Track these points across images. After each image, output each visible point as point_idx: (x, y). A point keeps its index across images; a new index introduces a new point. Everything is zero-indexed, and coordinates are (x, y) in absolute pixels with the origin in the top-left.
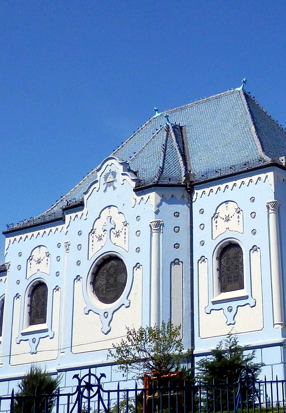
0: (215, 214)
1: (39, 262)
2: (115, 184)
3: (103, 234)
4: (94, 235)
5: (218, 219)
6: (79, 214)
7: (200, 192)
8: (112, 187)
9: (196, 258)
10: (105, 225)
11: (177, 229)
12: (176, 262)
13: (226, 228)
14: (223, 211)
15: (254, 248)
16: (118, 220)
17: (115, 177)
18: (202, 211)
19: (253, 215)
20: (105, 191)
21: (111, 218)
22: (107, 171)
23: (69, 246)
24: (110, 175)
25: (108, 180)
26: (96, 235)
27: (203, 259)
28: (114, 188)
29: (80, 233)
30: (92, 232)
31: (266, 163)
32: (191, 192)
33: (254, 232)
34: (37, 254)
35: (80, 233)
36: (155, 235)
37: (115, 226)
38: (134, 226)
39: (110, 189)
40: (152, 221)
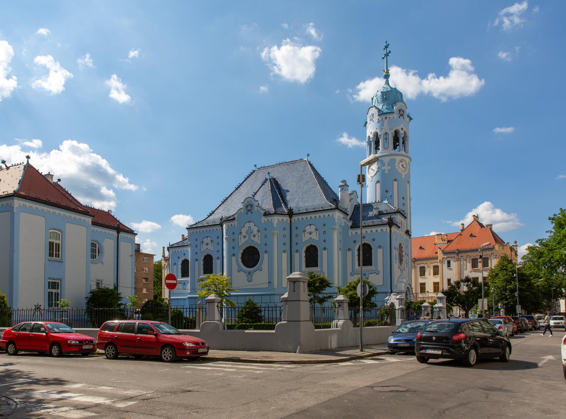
1: (207, 244)
5: (306, 233)
6: (233, 223)
9: (294, 250)
11: (284, 236)
12: (284, 251)
14: (308, 229)
15: (325, 249)
16: (255, 229)
17: (252, 207)
19: (324, 232)
25: (248, 208)
27: (297, 251)
29: (233, 233)
30: (241, 233)
31: (332, 207)
32: (291, 217)
33: (325, 241)
34: (206, 241)
35: (233, 233)
39: (250, 213)
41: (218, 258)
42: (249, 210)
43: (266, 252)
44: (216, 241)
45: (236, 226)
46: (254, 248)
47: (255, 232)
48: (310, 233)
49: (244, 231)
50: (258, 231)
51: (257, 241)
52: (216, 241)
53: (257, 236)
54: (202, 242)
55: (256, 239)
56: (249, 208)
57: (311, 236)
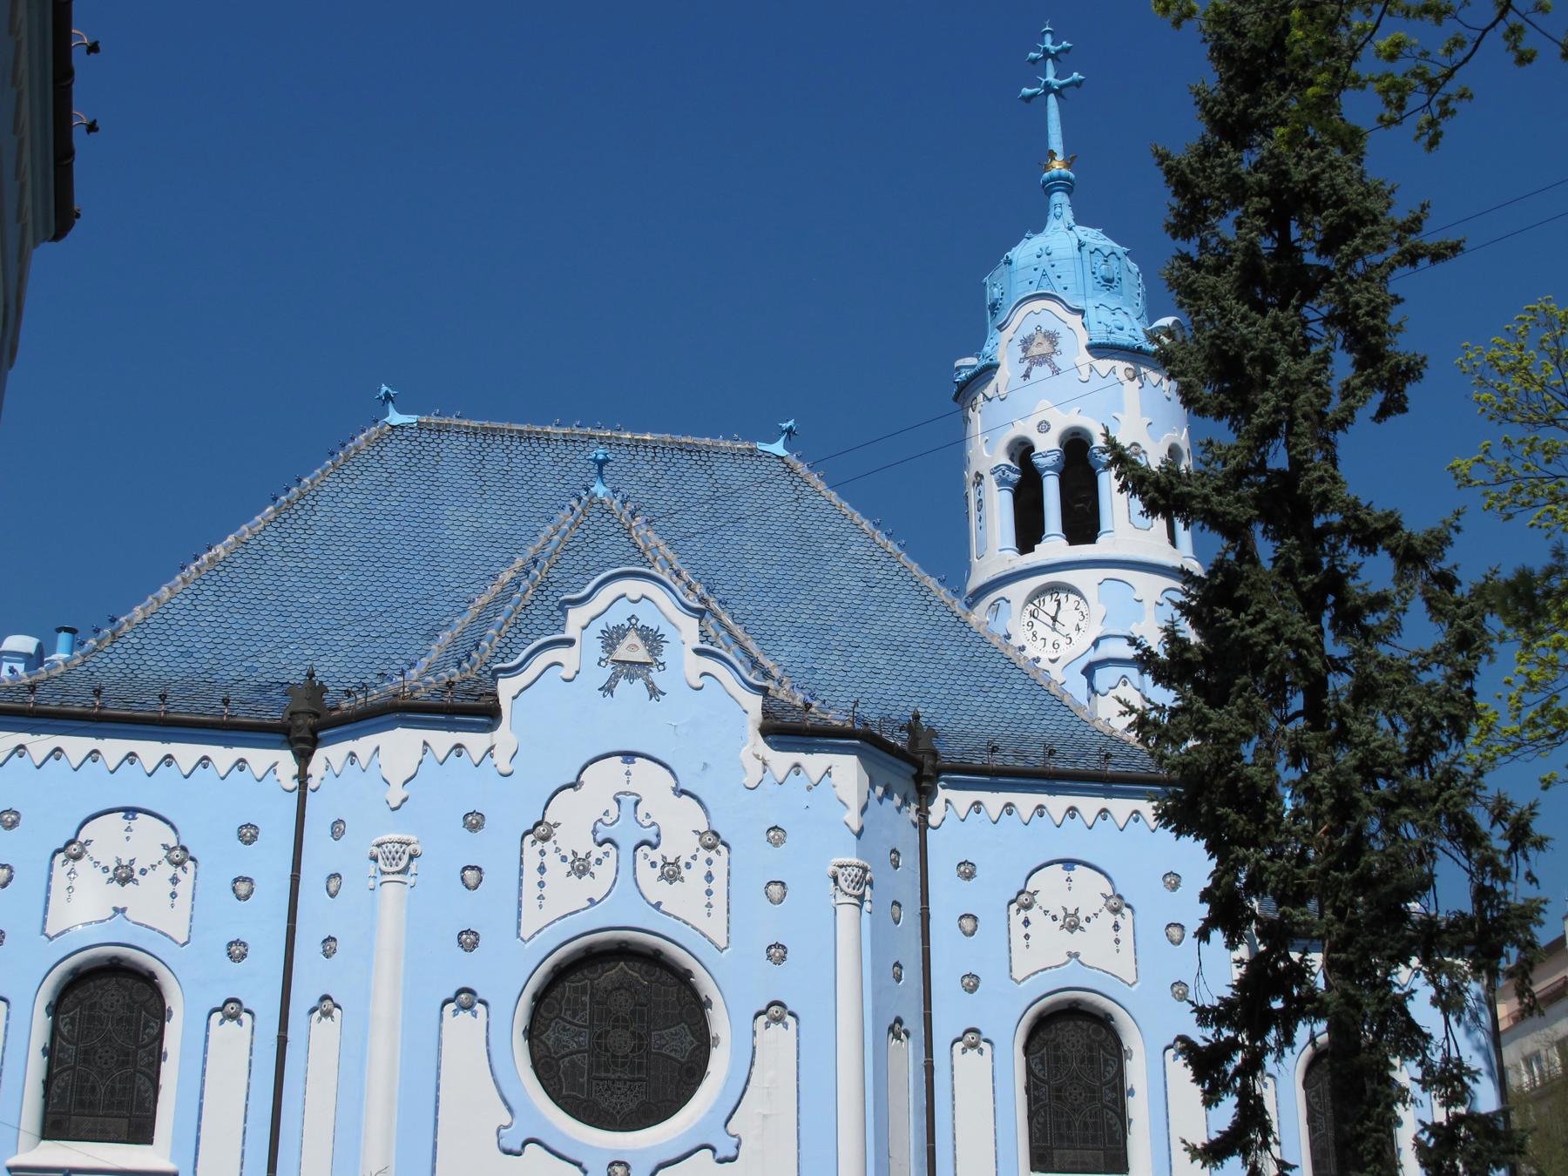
0: (1021, 892)
1: (124, 876)
2: (655, 675)
3: (597, 852)
4: (549, 846)
6: (475, 742)
7: (963, 799)
8: (639, 683)
10: (607, 820)
12: (896, 1029)
13: (1069, 954)
18: (967, 871)
20: (608, 689)
21: (637, 804)
22: (617, 617)
23: (412, 857)
24: (632, 638)
25: (622, 653)
26: (558, 850)
27: (972, 1038)
28: (654, 692)
30: (541, 831)
34: (107, 839)
36: (847, 913)
37: (658, 835)
38: (755, 859)
39: (631, 691)
40: (847, 860)
41: (232, 1009)
42: (631, 669)
43: (776, 1012)
44: (221, 858)
45: (502, 760)
46: (653, 960)
47: (680, 842)
48: (1072, 924)
49: (574, 820)
50: (713, 840)
51: (689, 917)
52: (221, 858)
53: (694, 877)
54: (72, 850)
55: (684, 899)
56: (632, 649)
57: (1074, 941)
